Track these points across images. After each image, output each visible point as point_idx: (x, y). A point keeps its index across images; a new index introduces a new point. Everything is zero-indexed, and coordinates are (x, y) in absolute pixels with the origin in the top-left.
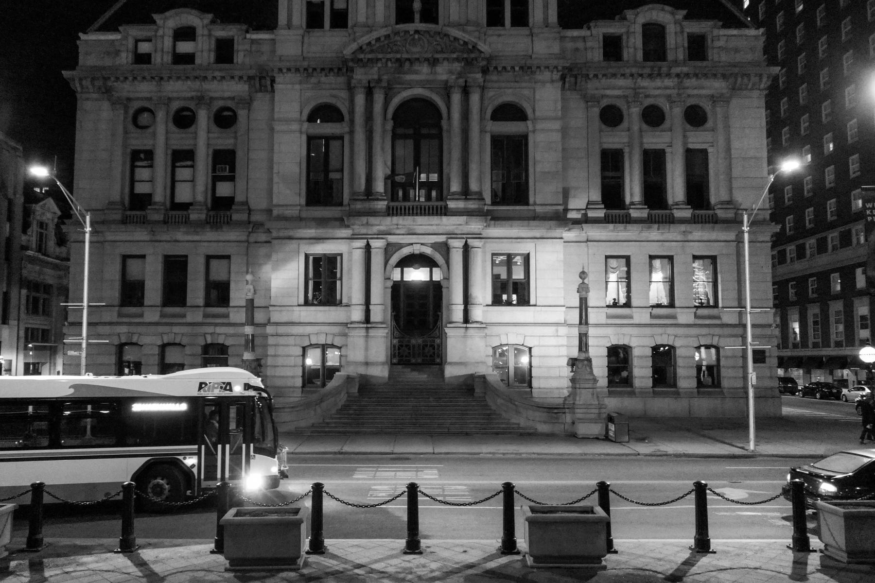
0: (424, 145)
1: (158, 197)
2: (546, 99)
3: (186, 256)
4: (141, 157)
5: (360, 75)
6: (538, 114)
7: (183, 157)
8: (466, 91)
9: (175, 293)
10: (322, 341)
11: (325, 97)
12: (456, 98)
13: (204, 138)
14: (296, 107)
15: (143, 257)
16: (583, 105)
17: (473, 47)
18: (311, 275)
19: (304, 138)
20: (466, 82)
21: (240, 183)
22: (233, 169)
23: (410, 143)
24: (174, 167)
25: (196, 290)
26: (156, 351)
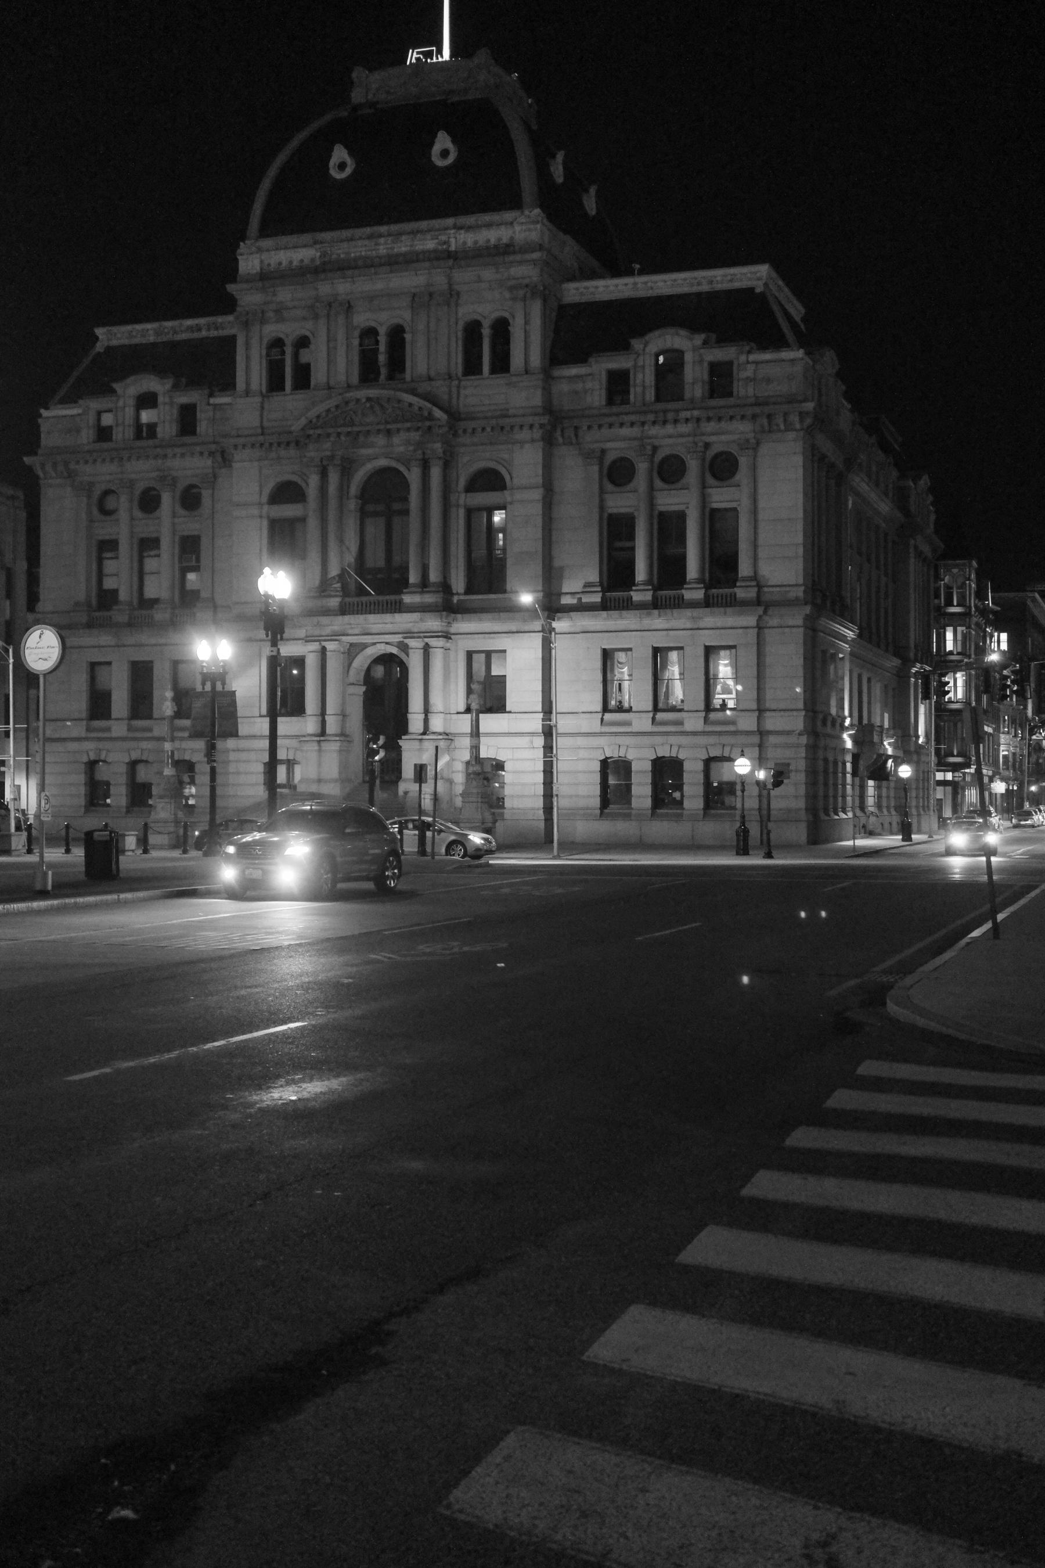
0: (396, 520)
6: (515, 481)
7: (148, 545)
13: (168, 522)
19: (265, 523)
20: (424, 453)
22: (198, 560)
23: (381, 522)
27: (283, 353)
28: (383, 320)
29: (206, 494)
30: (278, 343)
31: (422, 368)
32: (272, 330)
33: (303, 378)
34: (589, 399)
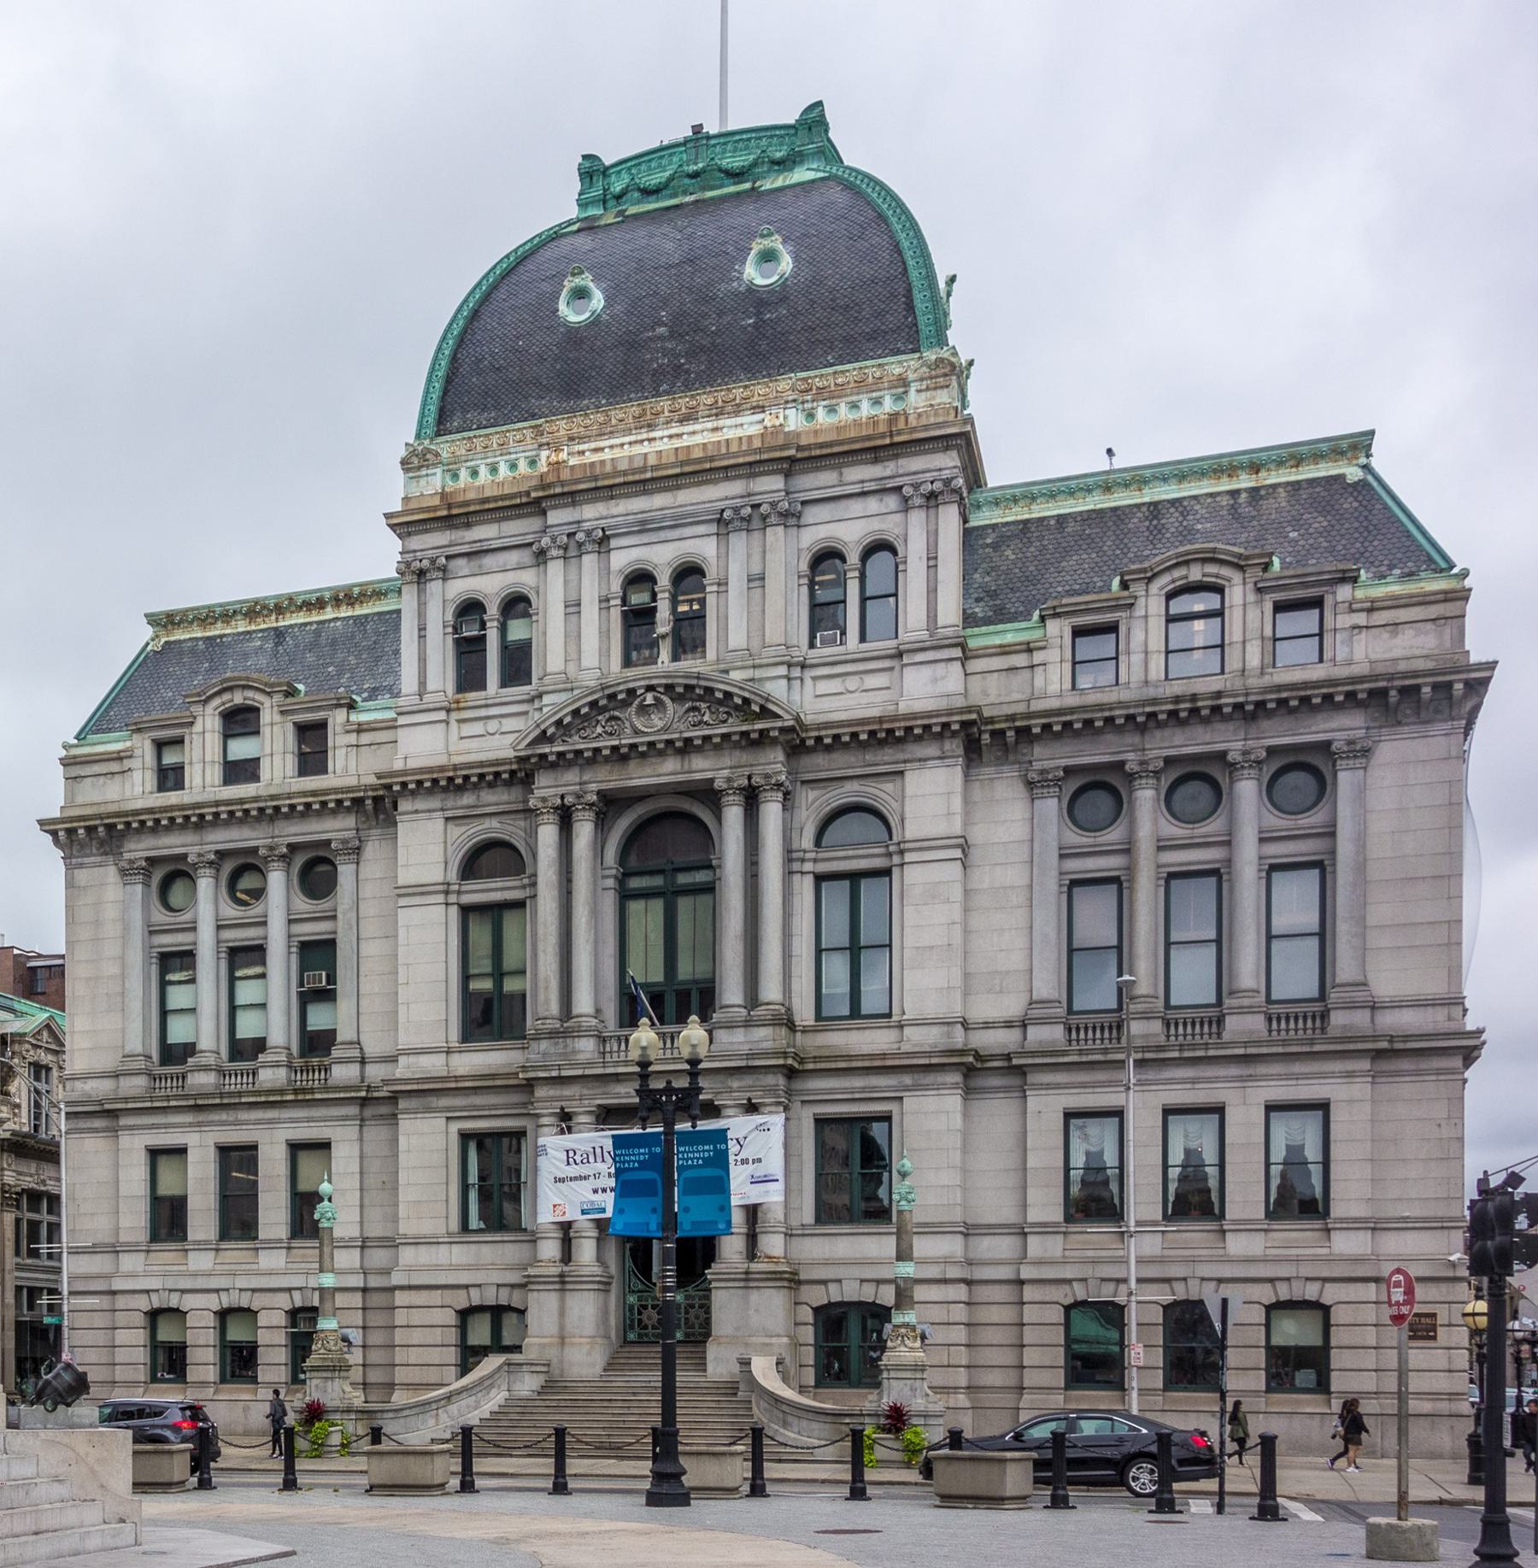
1: (206, 1042)
2: (929, 795)
3: (255, 1147)
4: (174, 963)
5: (547, 787)
7: (245, 956)
8: (751, 798)
9: (238, 1220)
10: (491, 1301)
11: (492, 828)
12: (733, 815)
14: (437, 852)
15: (181, 1151)
16: (1020, 791)
17: (762, 707)
18: (473, 1178)
19: (454, 911)
21: (345, 1005)
22: (332, 979)
23: (657, 905)
24: (232, 980)
25: (274, 1214)
26: (211, 1320)
27: (483, 626)
28: (662, 557)
29: (345, 872)
30: (471, 608)
31: (737, 639)
32: (461, 587)
33: (518, 664)
34: (1039, 681)
